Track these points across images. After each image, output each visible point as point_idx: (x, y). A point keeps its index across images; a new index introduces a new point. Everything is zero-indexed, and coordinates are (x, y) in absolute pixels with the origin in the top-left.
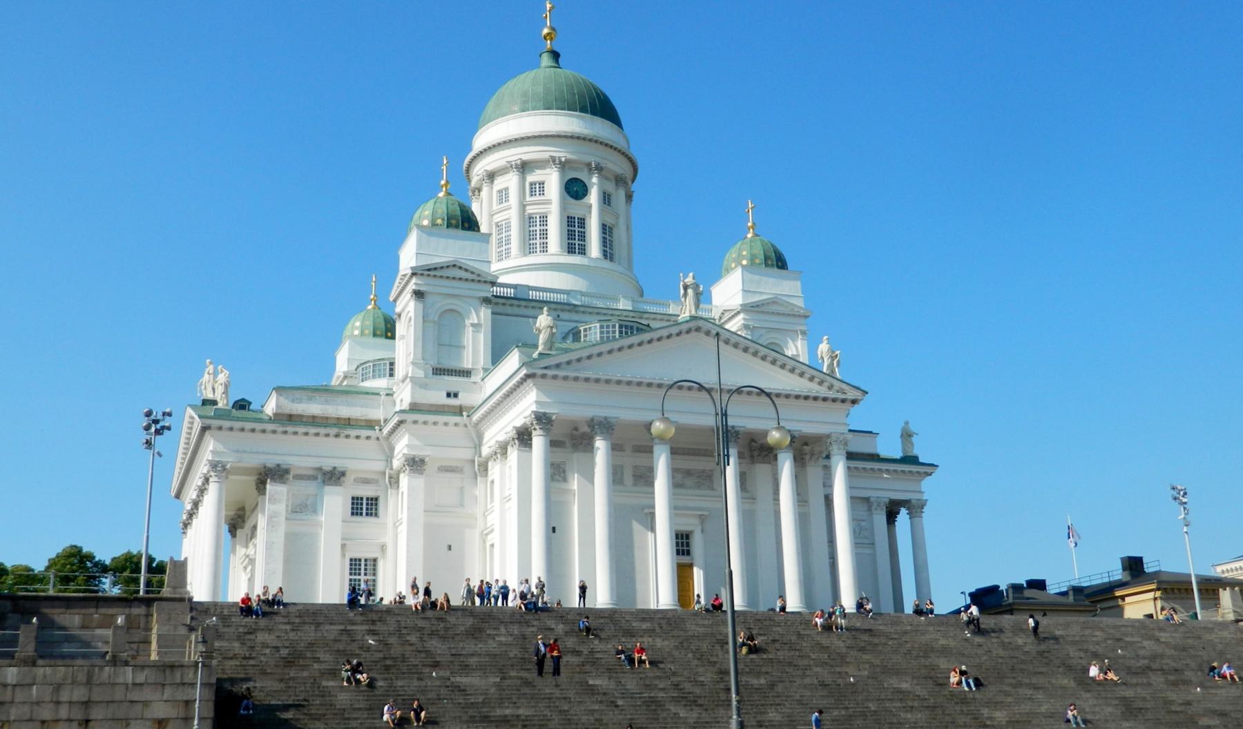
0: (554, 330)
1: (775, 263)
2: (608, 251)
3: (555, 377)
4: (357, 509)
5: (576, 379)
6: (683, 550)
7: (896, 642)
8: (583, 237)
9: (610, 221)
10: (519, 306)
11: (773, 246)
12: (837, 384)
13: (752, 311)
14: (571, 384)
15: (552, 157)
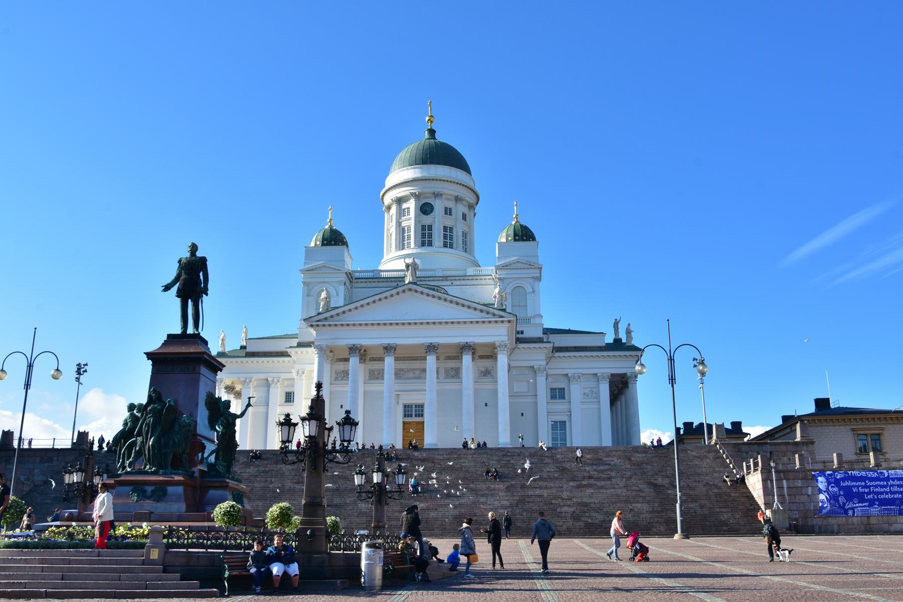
0: (328, 300)
1: (520, 238)
2: (448, 243)
3: (324, 325)
4: (288, 398)
5: (336, 325)
6: (419, 414)
7: (433, 465)
8: (430, 236)
9: (449, 222)
10: (374, 282)
11: (521, 226)
12: (497, 312)
13: (504, 269)
14: (333, 328)
15: (412, 194)
